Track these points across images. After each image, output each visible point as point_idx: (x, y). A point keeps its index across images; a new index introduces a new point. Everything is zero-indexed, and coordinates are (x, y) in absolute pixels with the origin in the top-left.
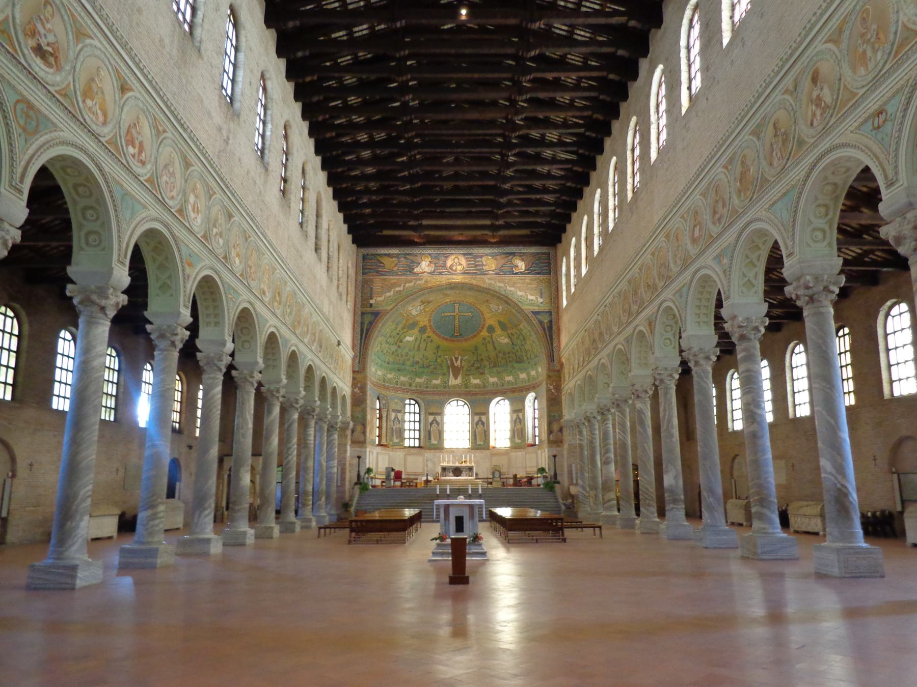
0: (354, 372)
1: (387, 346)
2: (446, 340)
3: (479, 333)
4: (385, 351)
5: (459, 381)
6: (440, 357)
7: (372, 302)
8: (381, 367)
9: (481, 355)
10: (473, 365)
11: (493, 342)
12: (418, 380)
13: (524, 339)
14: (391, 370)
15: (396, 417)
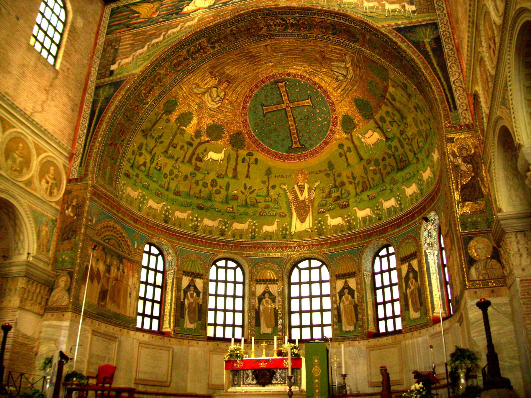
0: (69, 181)
1: (171, 163)
2: (280, 157)
3: (330, 137)
4: (166, 171)
5: (308, 224)
6: (274, 187)
7: (113, 67)
8: (158, 194)
9: (339, 175)
10: (329, 195)
11: (355, 147)
12: (237, 226)
13: (403, 117)
14: (185, 206)
15: (192, 285)
